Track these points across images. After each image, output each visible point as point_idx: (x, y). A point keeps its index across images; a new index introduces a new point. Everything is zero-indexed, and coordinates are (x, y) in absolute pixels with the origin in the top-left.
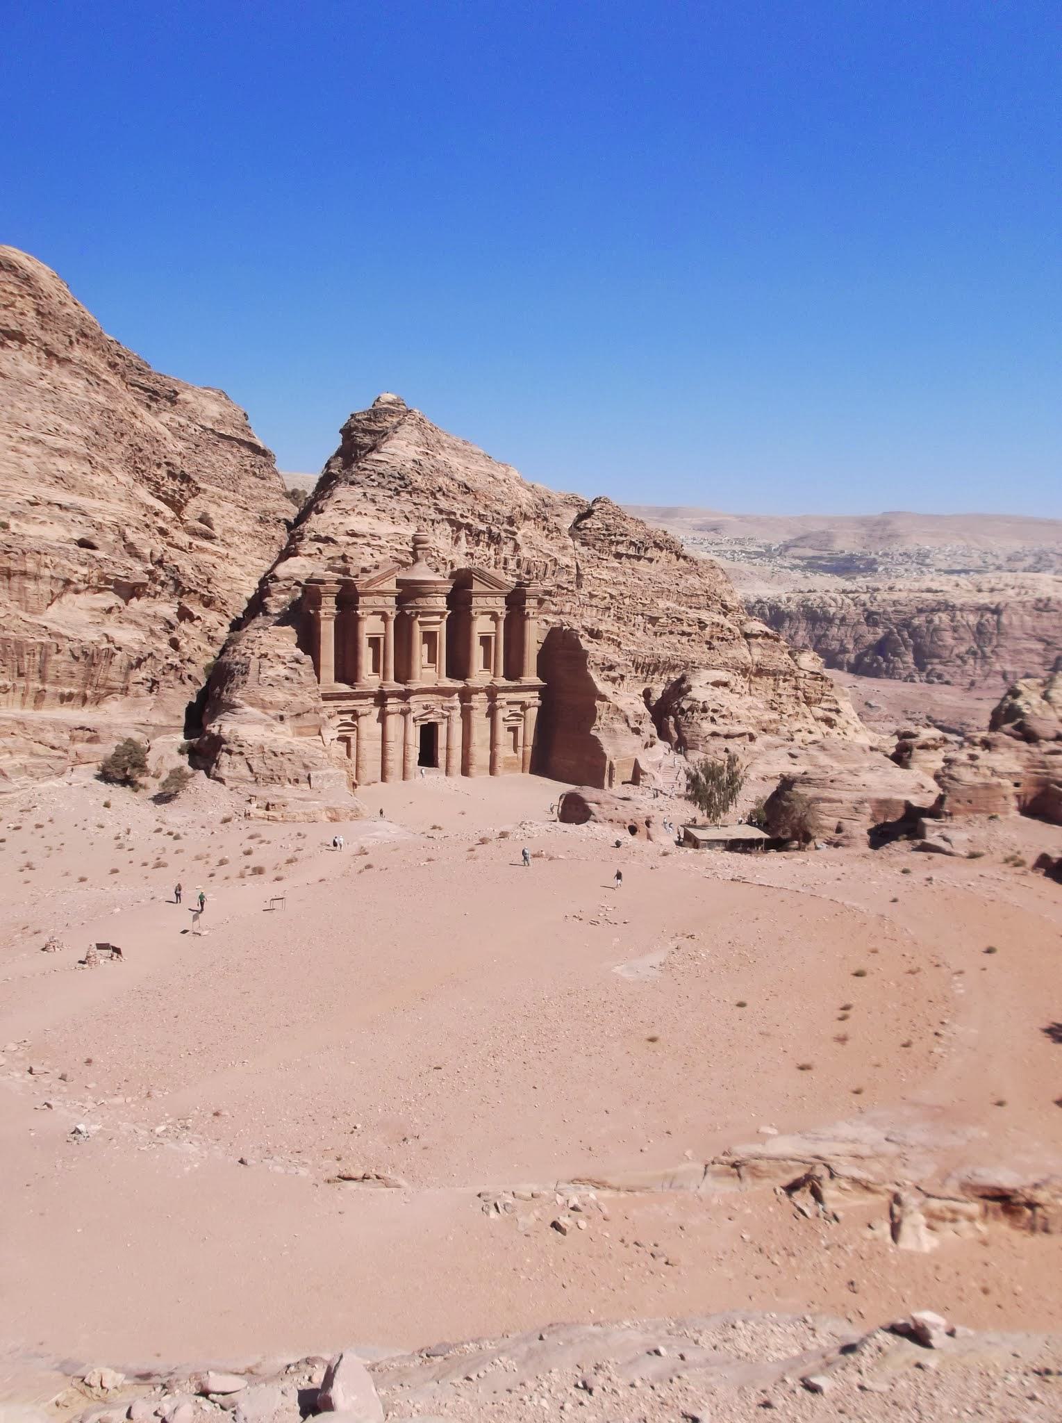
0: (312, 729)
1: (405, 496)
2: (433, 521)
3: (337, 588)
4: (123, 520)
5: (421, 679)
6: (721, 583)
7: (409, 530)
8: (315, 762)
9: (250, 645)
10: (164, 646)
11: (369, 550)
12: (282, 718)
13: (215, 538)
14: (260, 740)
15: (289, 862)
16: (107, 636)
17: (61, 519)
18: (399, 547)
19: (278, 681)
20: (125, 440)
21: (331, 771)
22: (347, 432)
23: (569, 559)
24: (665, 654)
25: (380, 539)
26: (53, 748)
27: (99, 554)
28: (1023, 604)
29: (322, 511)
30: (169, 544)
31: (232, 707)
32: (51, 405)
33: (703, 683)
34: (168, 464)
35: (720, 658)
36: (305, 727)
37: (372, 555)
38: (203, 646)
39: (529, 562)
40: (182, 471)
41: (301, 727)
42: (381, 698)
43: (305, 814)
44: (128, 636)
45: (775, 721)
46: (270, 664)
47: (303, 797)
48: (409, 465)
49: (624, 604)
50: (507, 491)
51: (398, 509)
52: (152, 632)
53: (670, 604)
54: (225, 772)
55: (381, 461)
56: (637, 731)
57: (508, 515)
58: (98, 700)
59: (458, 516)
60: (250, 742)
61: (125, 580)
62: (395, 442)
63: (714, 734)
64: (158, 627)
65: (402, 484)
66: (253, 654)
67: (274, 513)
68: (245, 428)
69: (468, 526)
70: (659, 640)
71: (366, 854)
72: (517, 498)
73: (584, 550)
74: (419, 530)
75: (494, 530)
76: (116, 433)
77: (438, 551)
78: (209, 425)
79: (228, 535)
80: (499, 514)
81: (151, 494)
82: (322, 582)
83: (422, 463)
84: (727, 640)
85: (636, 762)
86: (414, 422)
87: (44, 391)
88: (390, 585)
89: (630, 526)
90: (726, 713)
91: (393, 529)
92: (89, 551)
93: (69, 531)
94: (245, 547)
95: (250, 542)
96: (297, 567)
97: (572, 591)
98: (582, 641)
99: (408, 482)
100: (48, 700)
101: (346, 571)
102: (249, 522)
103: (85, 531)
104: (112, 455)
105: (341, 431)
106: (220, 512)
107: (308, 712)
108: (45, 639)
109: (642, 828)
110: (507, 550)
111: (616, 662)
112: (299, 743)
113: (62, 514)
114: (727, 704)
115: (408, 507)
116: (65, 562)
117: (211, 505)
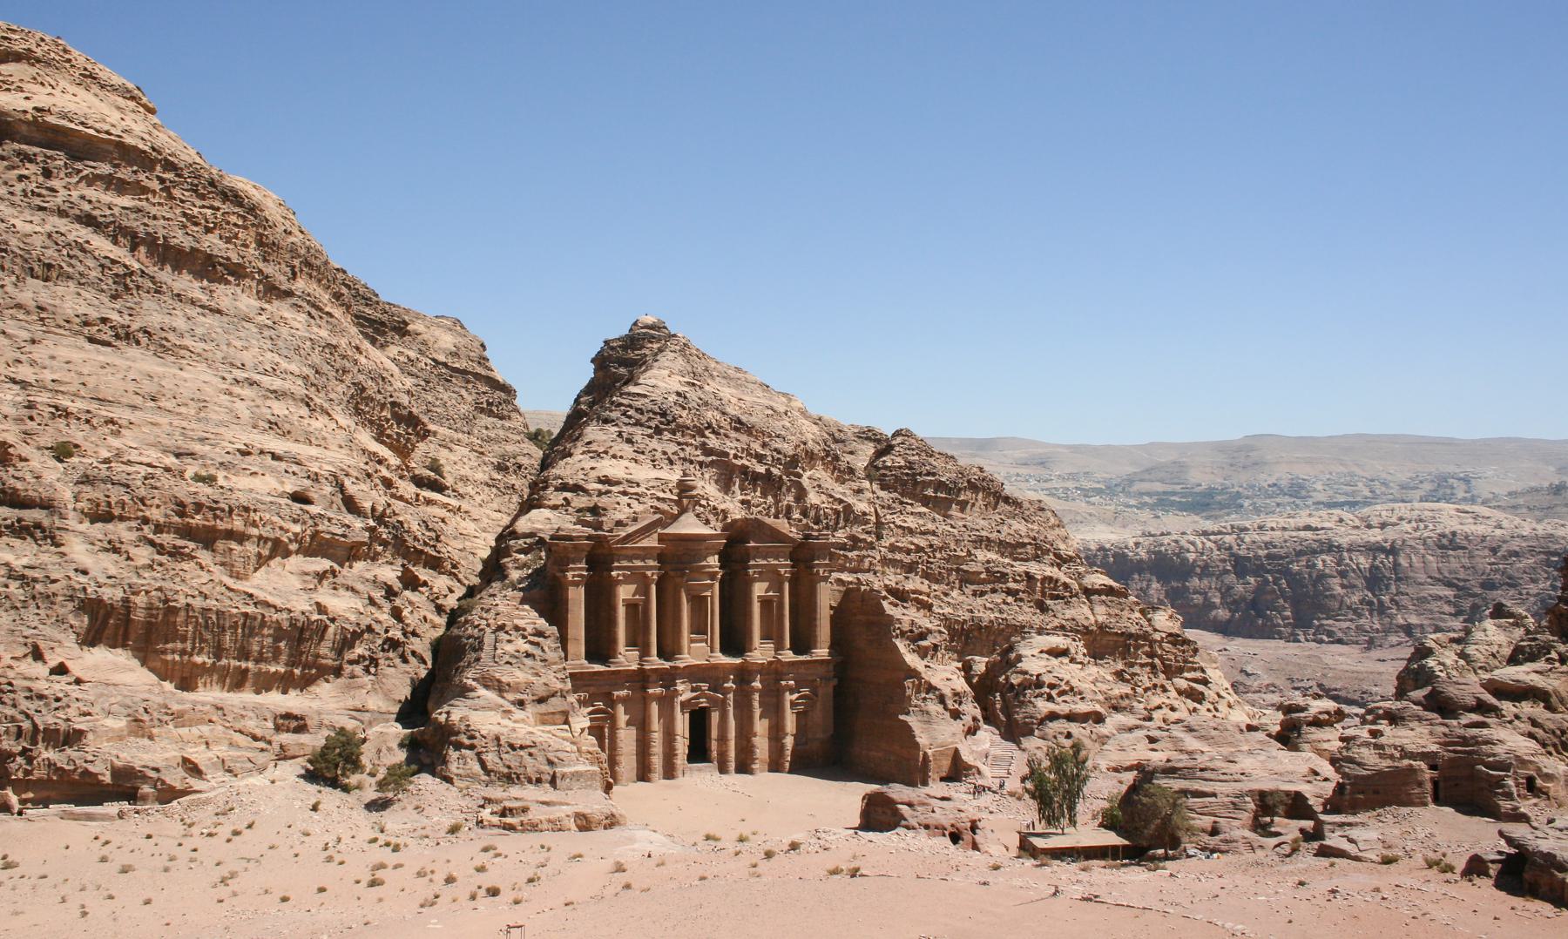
0: (557, 716)
1: (667, 435)
2: (701, 464)
4: (343, 470)
5: (689, 654)
6: (1052, 527)
7: (674, 476)
8: (561, 757)
9: (485, 615)
10: (385, 616)
12: (521, 704)
13: (447, 488)
14: (496, 729)
15: (531, 881)
16: (318, 604)
17: (273, 470)
18: (661, 495)
19: (517, 658)
20: (348, 379)
21: (581, 768)
22: (601, 361)
23: (866, 505)
25: (638, 485)
26: (255, 738)
27: (314, 509)
29: (570, 455)
30: (393, 496)
31: (464, 691)
32: (269, 342)
33: (1035, 652)
34: (394, 404)
35: (1056, 620)
36: (549, 714)
37: (629, 505)
38: (430, 616)
39: (817, 508)
40: (410, 412)
41: (545, 714)
43: (549, 821)
44: (343, 605)
45: (1127, 696)
46: (508, 637)
47: (547, 800)
48: (672, 398)
49: (935, 557)
50: (789, 425)
51: (660, 450)
52: (372, 602)
53: (992, 556)
54: (454, 767)
55: (639, 395)
56: (956, 715)
57: (791, 453)
58: (305, 683)
59: (731, 456)
60: (483, 732)
61: (343, 539)
62: (654, 372)
64: (378, 595)
65: (663, 421)
66: (488, 625)
67: (514, 458)
68: (483, 360)
70: (980, 601)
71: (624, 871)
72: (800, 433)
74: (685, 475)
75: (775, 471)
76: (337, 371)
77: (707, 499)
78: (442, 358)
79: (460, 484)
80: (779, 453)
81: (377, 440)
82: (570, 538)
83: (688, 395)
84: (1063, 598)
85: (956, 751)
86: (678, 348)
87: (261, 327)
89: (938, 463)
90: (1067, 688)
93: (283, 483)
94: (481, 498)
95: (486, 492)
96: (540, 521)
97: (872, 543)
98: (885, 604)
99: (670, 418)
101: (598, 526)
102: (485, 468)
103: (299, 483)
104: (332, 396)
105: (593, 361)
106: (453, 458)
107: (553, 696)
108: (250, 609)
109: (967, 836)
110: (789, 499)
111: (927, 629)
112: (542, 734)
113: (276, 463)
114: (1067, 677)
117: (442, 449)
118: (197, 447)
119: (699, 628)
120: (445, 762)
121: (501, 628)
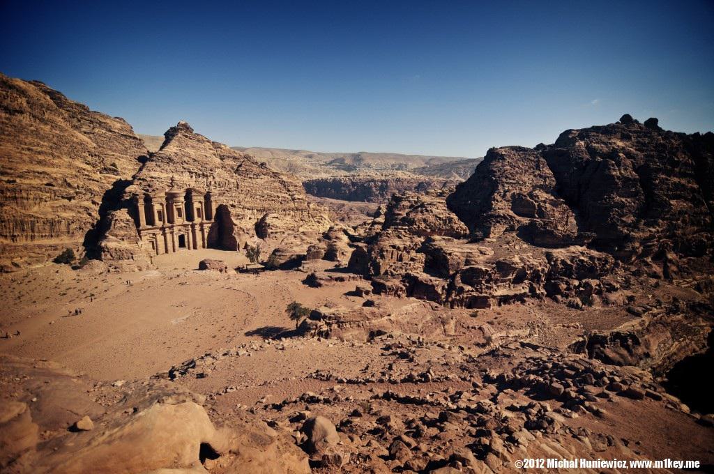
3: (144, 197)
10: (85, 216)
11: (158, 183)
12: (123, 240)
24: (267, 206)
27: (55, 188)
28: (393, 179)
42: (163, 229)
52: (79, 212)
54: (103, 257)
63: (272, 233)
68: (131, 132)
69: (196, 173)
73: (239, 177)
75: (205, 173)
78: (117, 131)
85: (246, 243)
87: (32, 131)
88: (163, 194)
91: (166, 176)
92: (51, 187)
100: (36, 237)
108: (32, 219)
113: (39, 175)
115: (172, 168)
116: (41, 193)
118: (9, 171)
119: (180, 215)
120: (101, 255)
121: (116, 220)
